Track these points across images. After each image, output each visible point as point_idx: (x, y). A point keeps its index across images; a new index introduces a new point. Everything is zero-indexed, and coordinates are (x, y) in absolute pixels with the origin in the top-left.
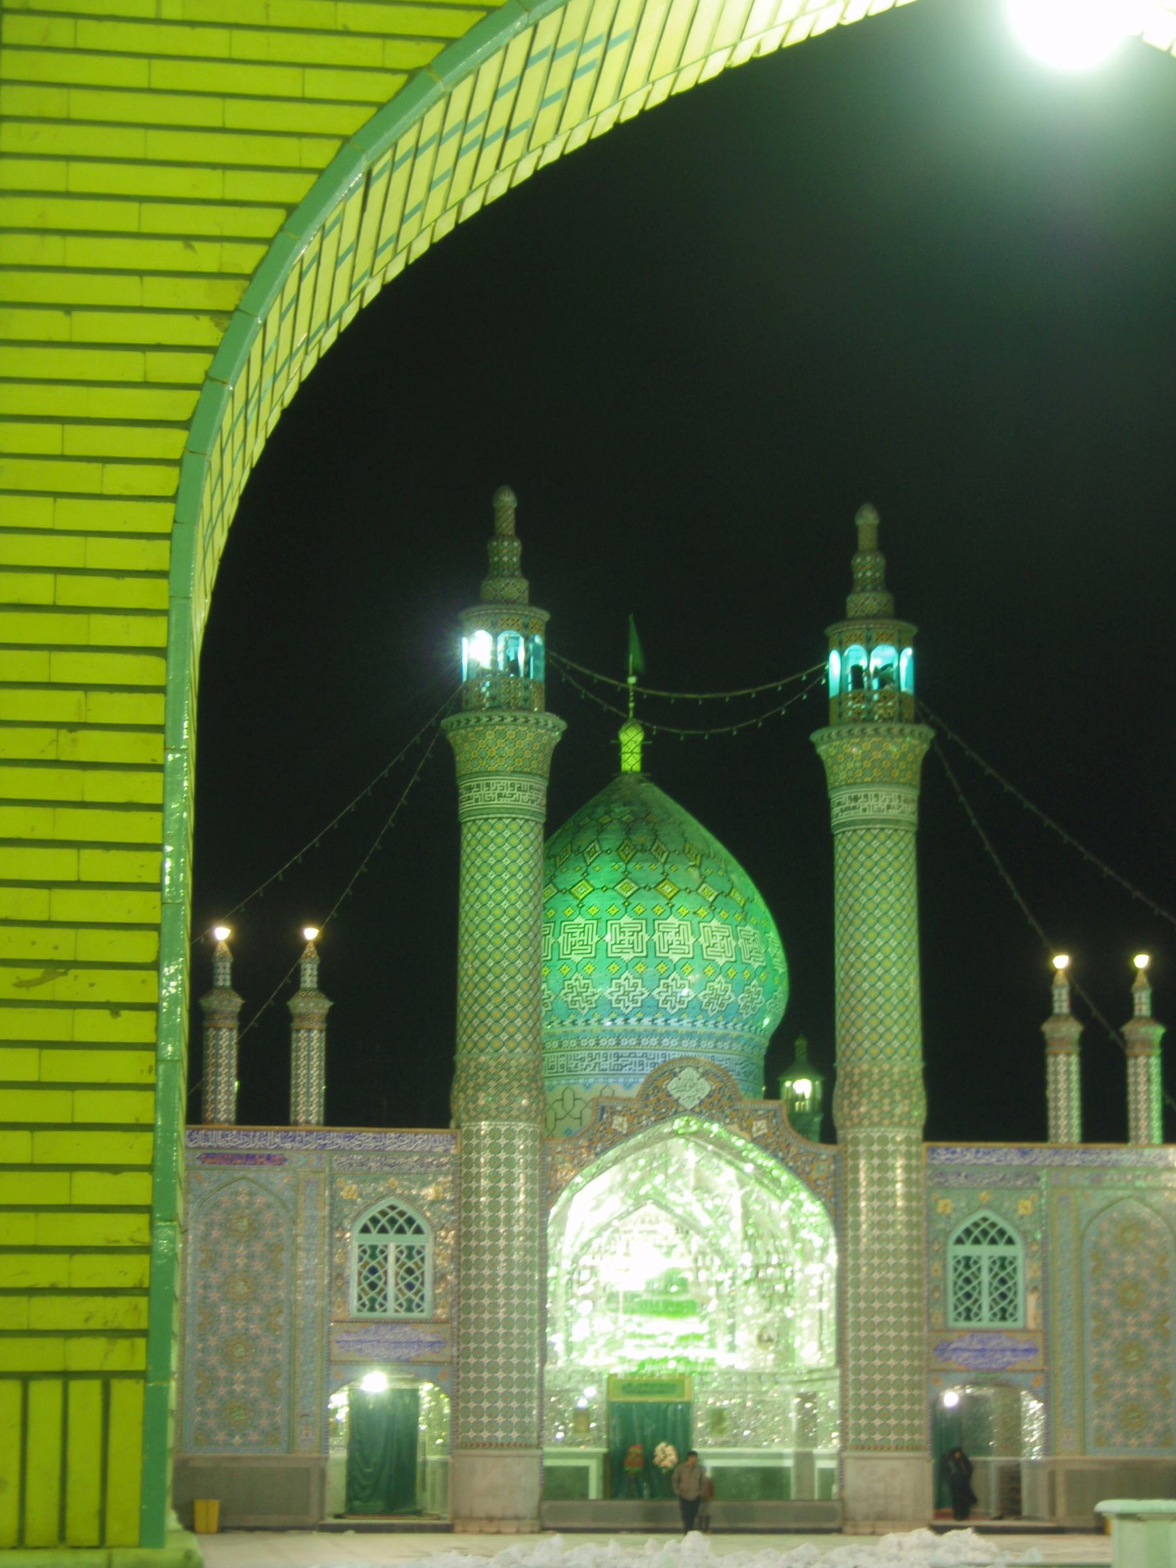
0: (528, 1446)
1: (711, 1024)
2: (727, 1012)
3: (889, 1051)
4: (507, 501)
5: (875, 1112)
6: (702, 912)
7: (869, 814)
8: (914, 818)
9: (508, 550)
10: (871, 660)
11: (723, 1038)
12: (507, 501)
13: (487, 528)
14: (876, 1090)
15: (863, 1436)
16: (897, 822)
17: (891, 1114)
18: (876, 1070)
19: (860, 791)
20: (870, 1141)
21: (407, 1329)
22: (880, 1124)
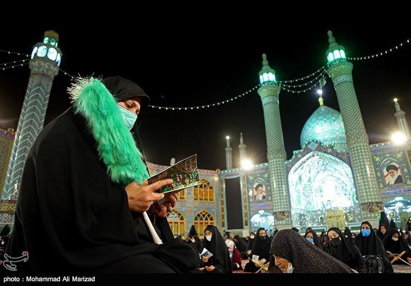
0: (289, 224)
1: (338, 141)
2: (341, 138)
3: (354, 127)
4: (264, 56)
5: (353, 141)
6: (332, 121)
7: (340, 82)
8: (352, 80)
9: (265, 62)
10: (336, 55)
11: (342, 143)
12: (264, 56)
13: (262, 60)
14: (353, 136)
15: (366, 216)
16: (346, 82)
17: (357, 141)
18: (352, 132)
19: (337, 78)
20: (354, 148)
21: (263, 203)
22: (355, 143)
